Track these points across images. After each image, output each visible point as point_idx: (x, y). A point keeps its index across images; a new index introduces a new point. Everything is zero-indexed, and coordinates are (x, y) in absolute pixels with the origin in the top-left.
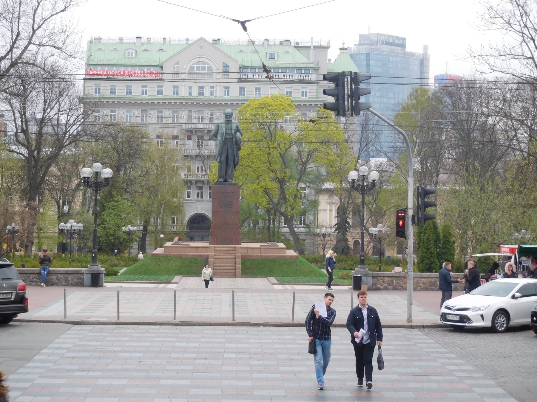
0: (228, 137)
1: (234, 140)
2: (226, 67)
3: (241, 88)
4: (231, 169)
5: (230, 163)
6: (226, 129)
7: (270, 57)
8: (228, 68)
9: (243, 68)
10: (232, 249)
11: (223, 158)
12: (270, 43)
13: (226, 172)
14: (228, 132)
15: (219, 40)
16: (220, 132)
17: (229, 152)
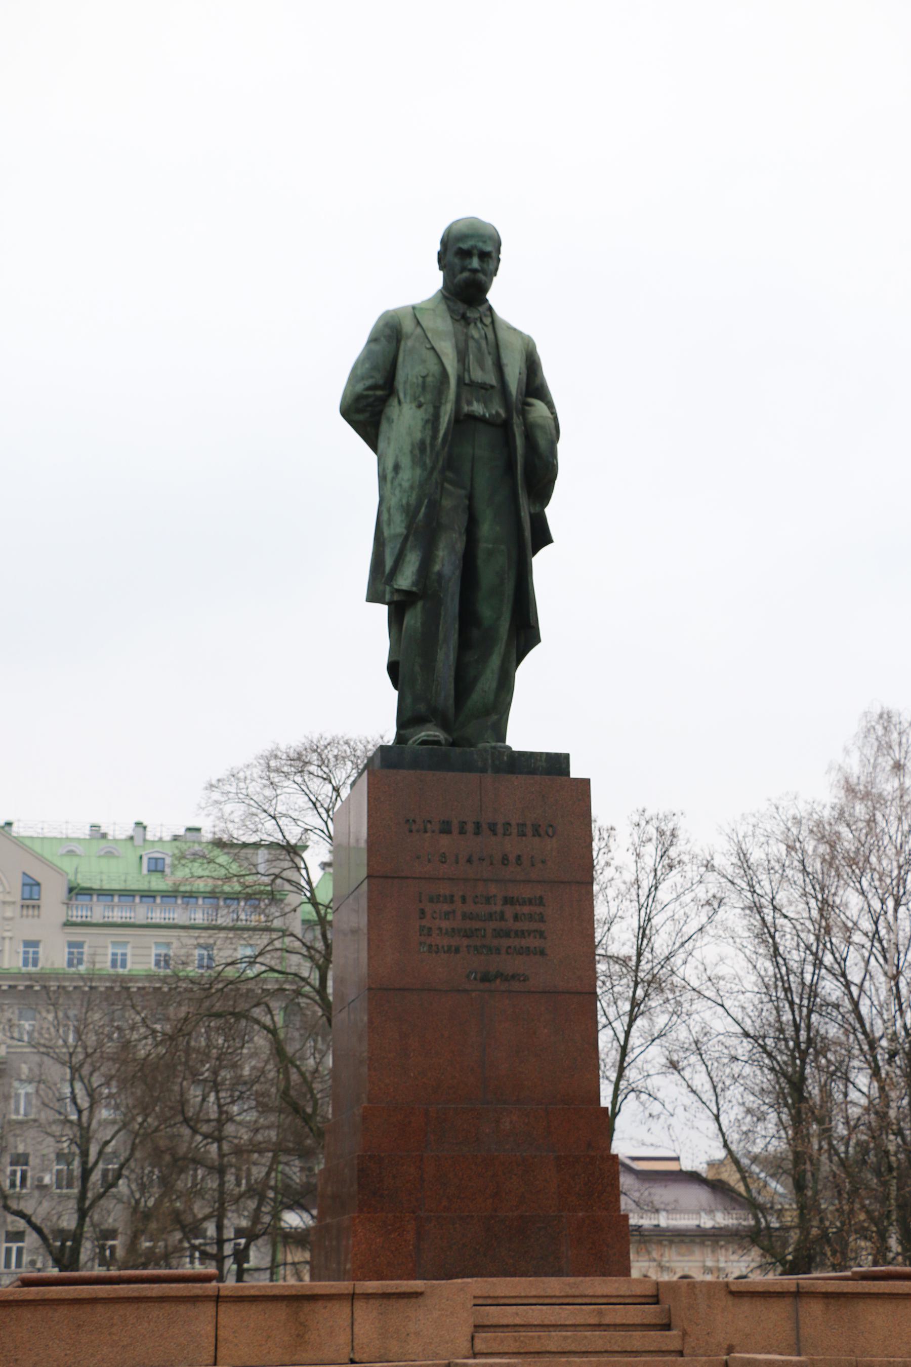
0: (477, 408)
1: (519, 442)
2: (31, 885)
3: (71, 945)
4: (495, 661)
5: (486, 611)
6: (462, 356)
7: (153, 868)
8: (35, 888)
9: (75, 891)
10: (634, 1314)
11: (446, 561)
12: (149, 836)
13: (463, 684)
14: (478, 375)
15: (9, 824)
16: (409, 372)
17: (486, 529)
